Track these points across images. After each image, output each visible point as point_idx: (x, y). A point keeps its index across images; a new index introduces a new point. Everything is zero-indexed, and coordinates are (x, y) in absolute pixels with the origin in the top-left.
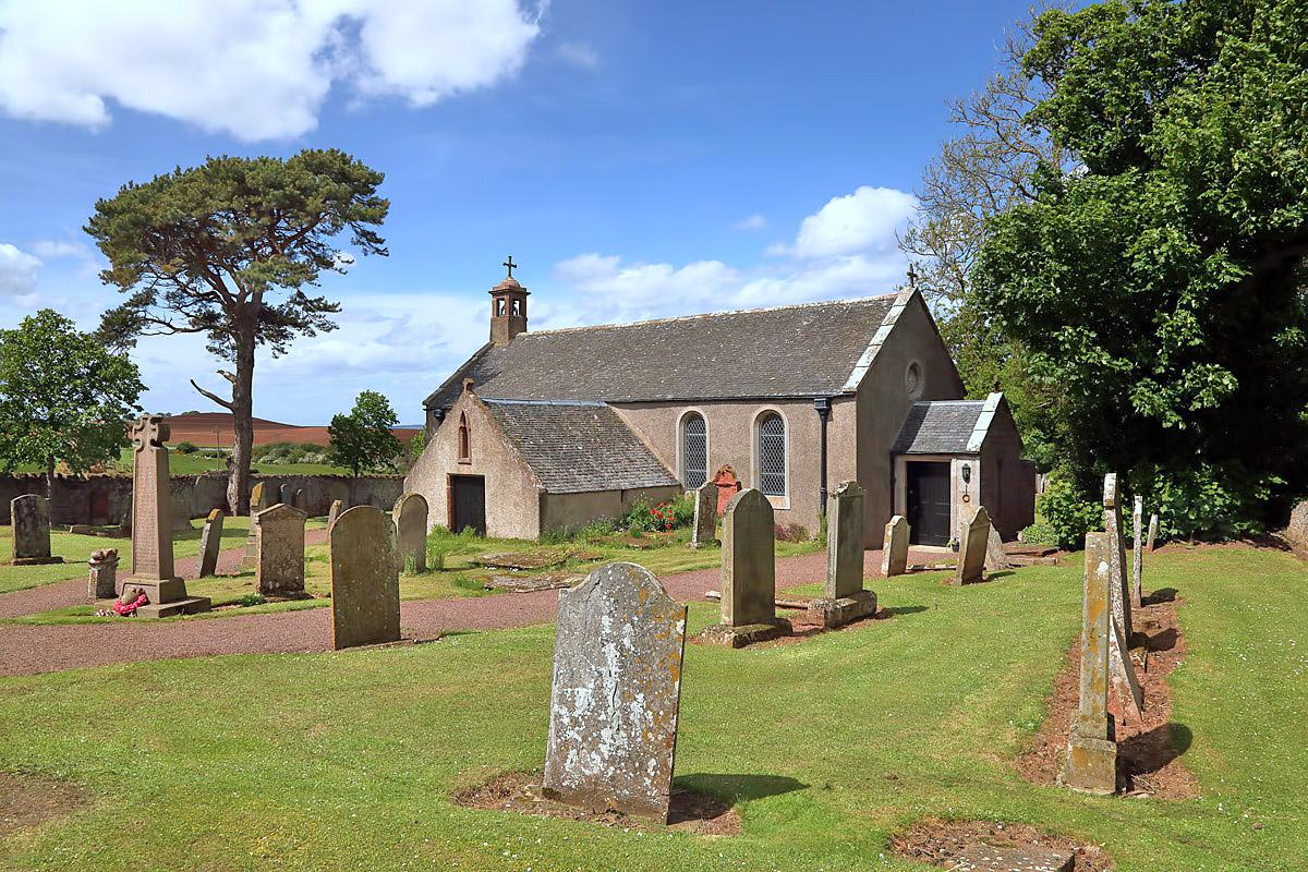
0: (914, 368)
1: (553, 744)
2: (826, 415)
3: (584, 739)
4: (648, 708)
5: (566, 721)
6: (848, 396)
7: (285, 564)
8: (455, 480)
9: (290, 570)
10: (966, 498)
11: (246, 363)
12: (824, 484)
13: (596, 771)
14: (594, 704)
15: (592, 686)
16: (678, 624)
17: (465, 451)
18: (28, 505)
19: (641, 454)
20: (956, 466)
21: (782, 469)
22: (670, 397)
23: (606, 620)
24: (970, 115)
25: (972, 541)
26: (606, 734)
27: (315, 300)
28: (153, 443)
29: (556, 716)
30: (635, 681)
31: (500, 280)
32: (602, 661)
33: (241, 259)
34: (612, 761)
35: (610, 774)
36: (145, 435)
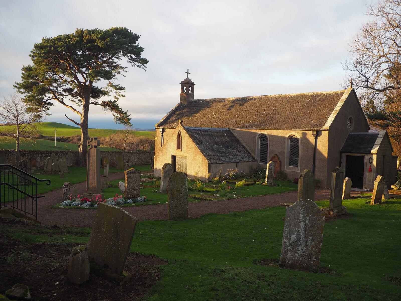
0: (350, 119)
1: (283, 251)
3: (293, 249)
4: (313, 241)
5: (287, 244)
6: (325, 130)
7: (134, 189)
9: (136, 191)
11: (86, 108)
13: (296, 259)
14: (296, 239)
15: (296, 234)
16: (323, 217)
17: (179, 146)
18: (24, 164)
19: (242, 149)
21: (297, 156)
23: (301, 215)
24: (376, 12)
25: (379, 188)
26: (300, 248)
28: (95, 147)
29: (284, 242)
30: (309, 233)
31: (183, 78)
32: (299, 227)
33: (82, 67)
34: (301, 256)
35: (301, 259)
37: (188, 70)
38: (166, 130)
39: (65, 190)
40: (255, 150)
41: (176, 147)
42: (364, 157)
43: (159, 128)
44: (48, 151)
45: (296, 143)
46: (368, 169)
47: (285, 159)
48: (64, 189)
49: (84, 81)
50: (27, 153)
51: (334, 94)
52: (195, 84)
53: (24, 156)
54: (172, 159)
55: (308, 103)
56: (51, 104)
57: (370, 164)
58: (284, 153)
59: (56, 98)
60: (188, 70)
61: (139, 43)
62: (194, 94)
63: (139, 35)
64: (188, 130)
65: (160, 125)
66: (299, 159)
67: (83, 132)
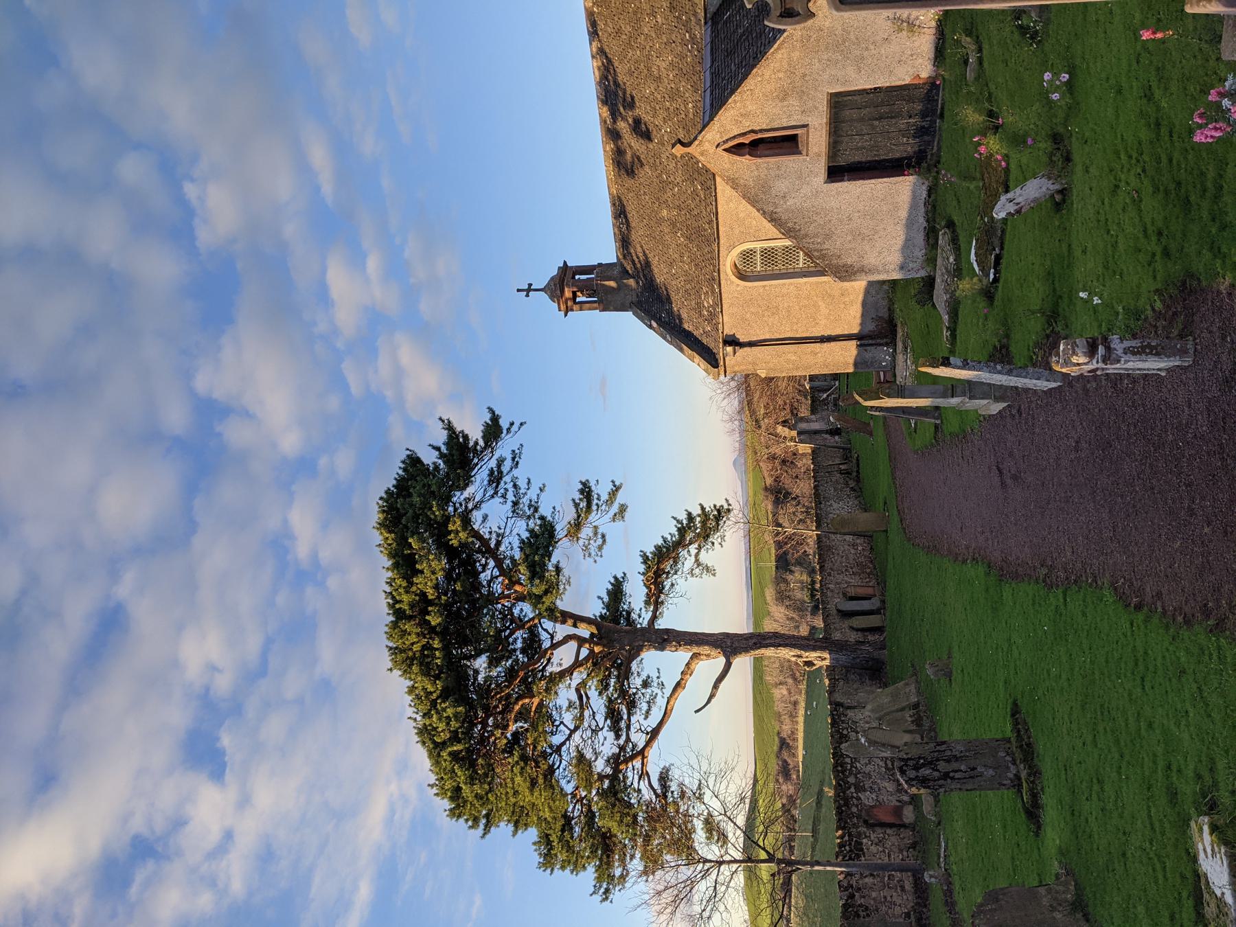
18: (917, 768)
37: (518, 290)
38: (728, 331)
39: (1127, 344)
41: (792, 158)
43: (722, 363)
44: (835, 766)
48: (1120, 352)
49: (573, 645)
50: (846, 838)
52: (565, 262)
53: (862, 850)
54: (842, 180)
56: (664, 778)
59: (642, 753)
60: (518, 290)
61: (430, 445)
62: (600, 265)
63: (408, 456)
64: (718, 95)
65: (711, 359)
67: (753, 649)
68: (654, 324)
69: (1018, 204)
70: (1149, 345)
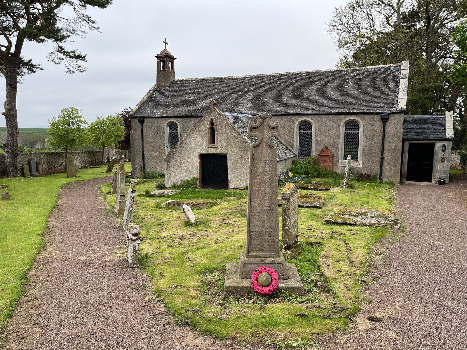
2: (385, 121)
8: (203, 157)
10: (443, 160)
12: (382, 154)
17: (213, 140)
20: (438, 146)
22: (291, 112)
27: (72, 52)
36: (262, 133)
37: (165, 38)
40: (293, 142)
42: (433, 146)
45: (354, 130)
46: (440, 159)
47: (339, 152)
48: (134, 244)
51: (384, 69)
52: (176, 59)
55: (353, 80)
57: (443, 153)
58: (338, 143)
62: (174, 72)
66: (359, 150)
68: (151, 92)
69: (187, 212)
70: (136, 253)
